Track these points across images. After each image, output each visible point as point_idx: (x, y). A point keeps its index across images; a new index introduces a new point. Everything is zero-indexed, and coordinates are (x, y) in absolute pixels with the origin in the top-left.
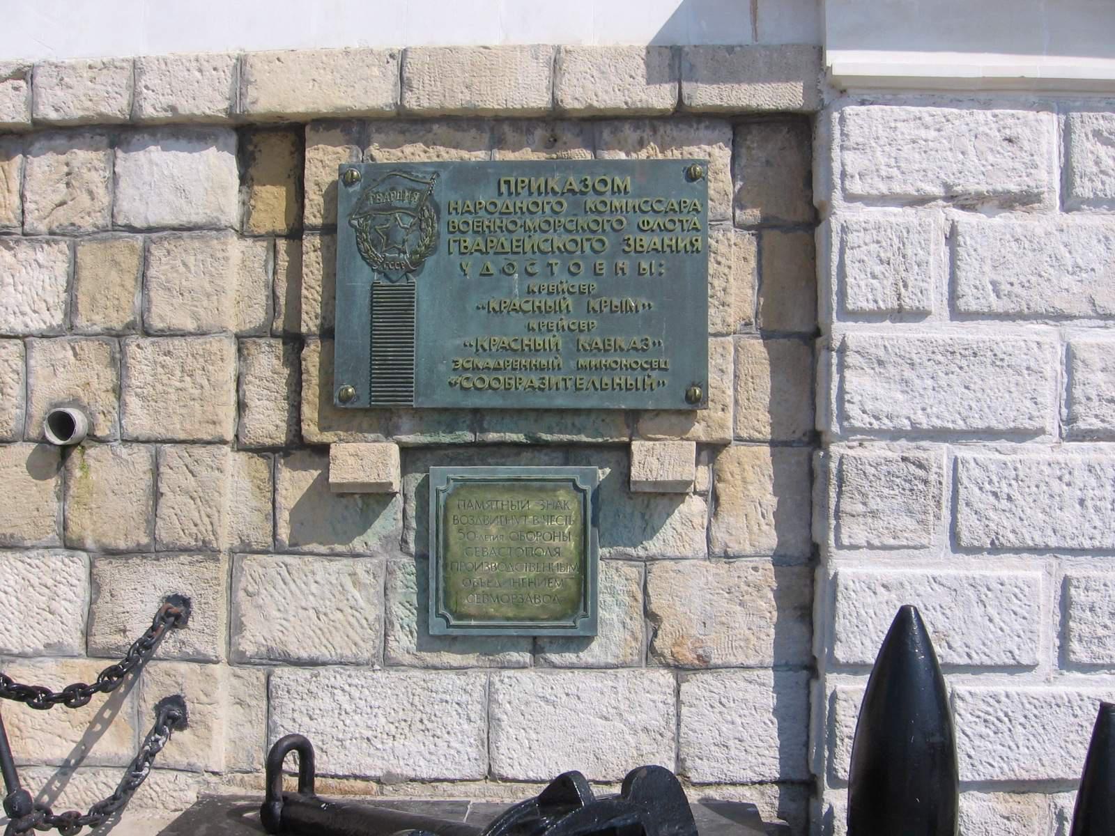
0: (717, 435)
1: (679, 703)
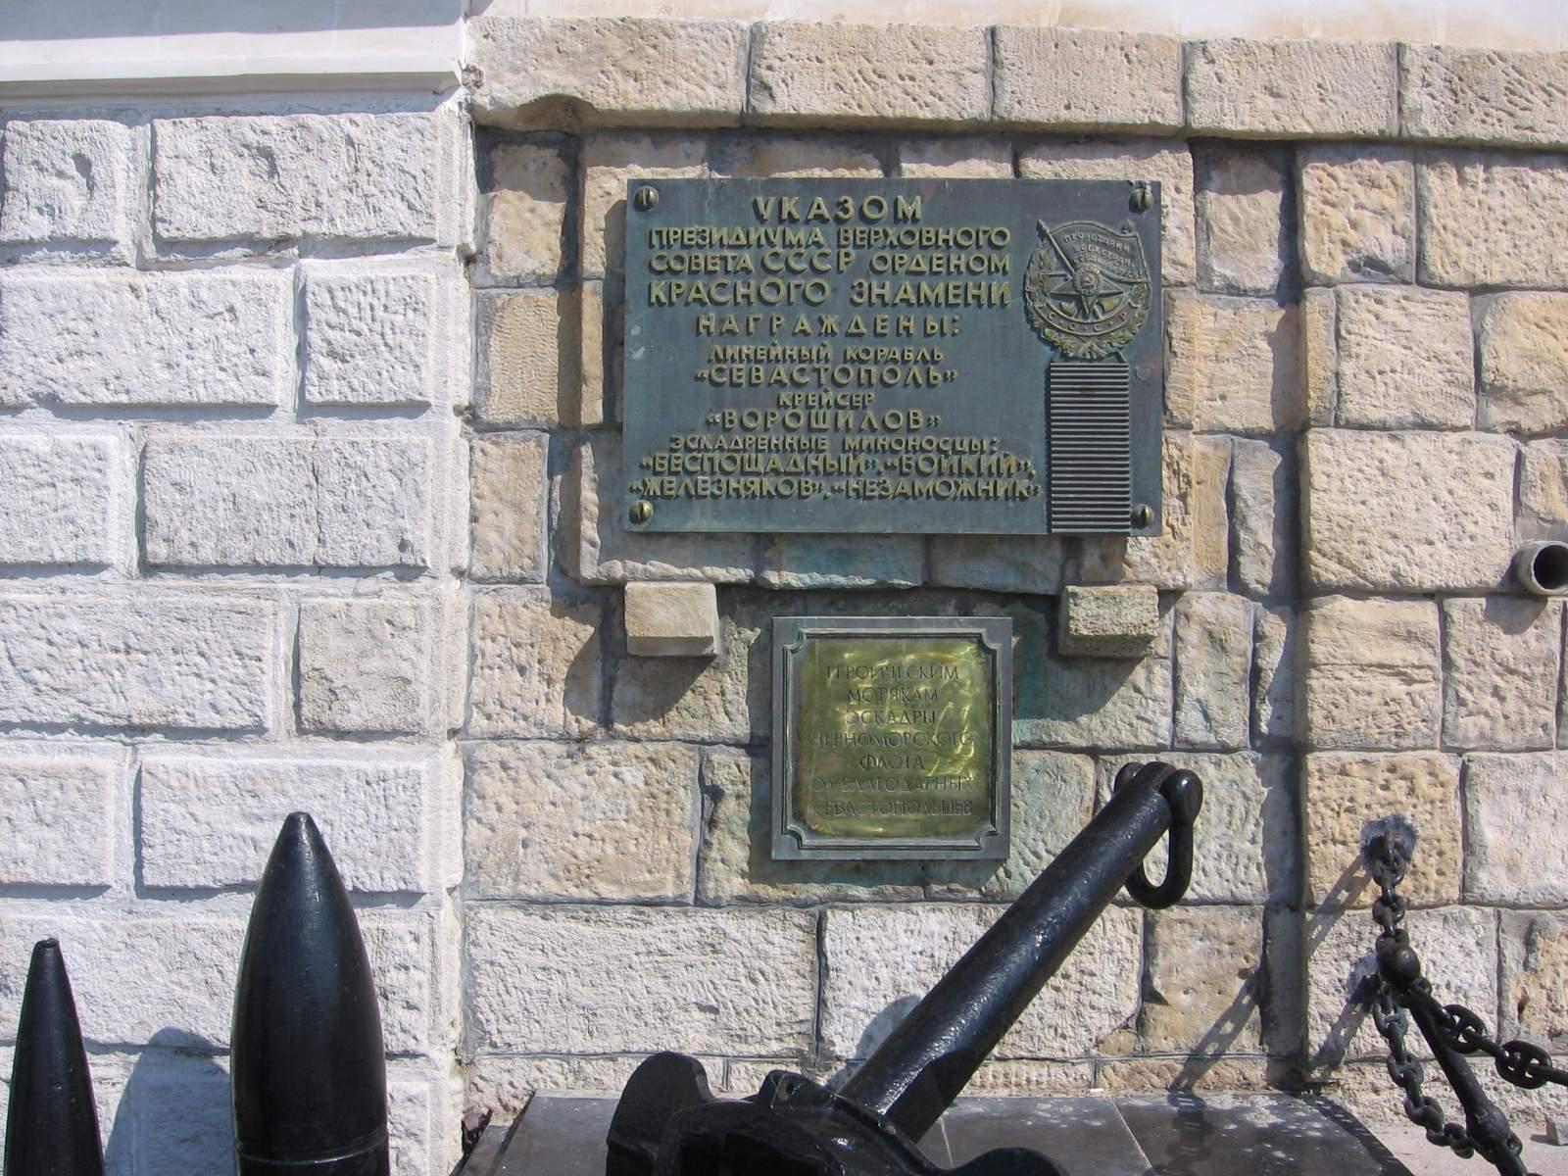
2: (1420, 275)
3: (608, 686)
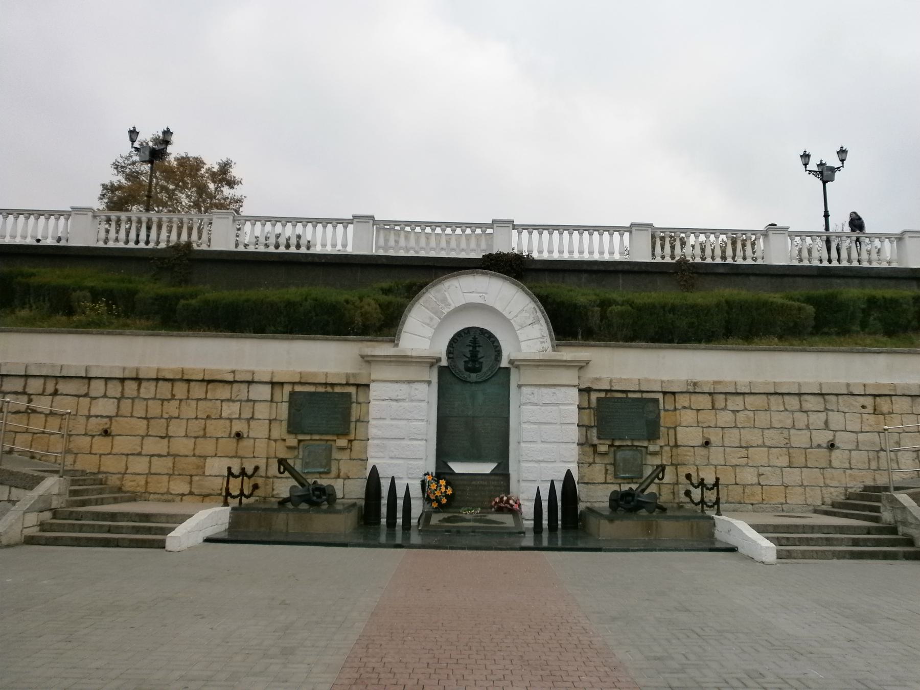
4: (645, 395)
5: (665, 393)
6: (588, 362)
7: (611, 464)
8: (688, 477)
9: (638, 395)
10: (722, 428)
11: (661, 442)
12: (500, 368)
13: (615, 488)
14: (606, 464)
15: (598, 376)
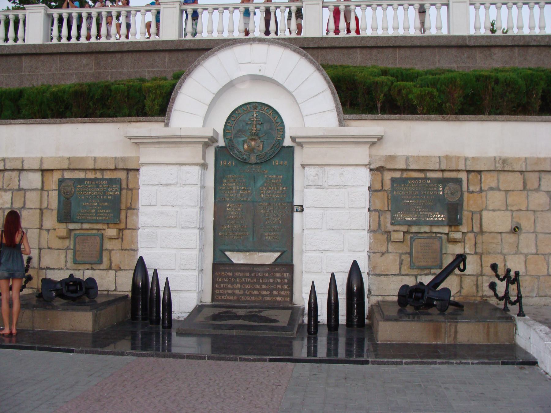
0: (121, 228)
1: (116, 276)
2: (498, 189)
3: (388, 244)
4: (447, 175)
5: (469, 172)
6: (380, 138)
7: (406, 253)
8: (494, 267)
9: (439, 175)
10: (534, 211)
11: (464, 229)
12: (284, 147)
13: (410, 282)
14: (401, 254)
15: (392, 154)
